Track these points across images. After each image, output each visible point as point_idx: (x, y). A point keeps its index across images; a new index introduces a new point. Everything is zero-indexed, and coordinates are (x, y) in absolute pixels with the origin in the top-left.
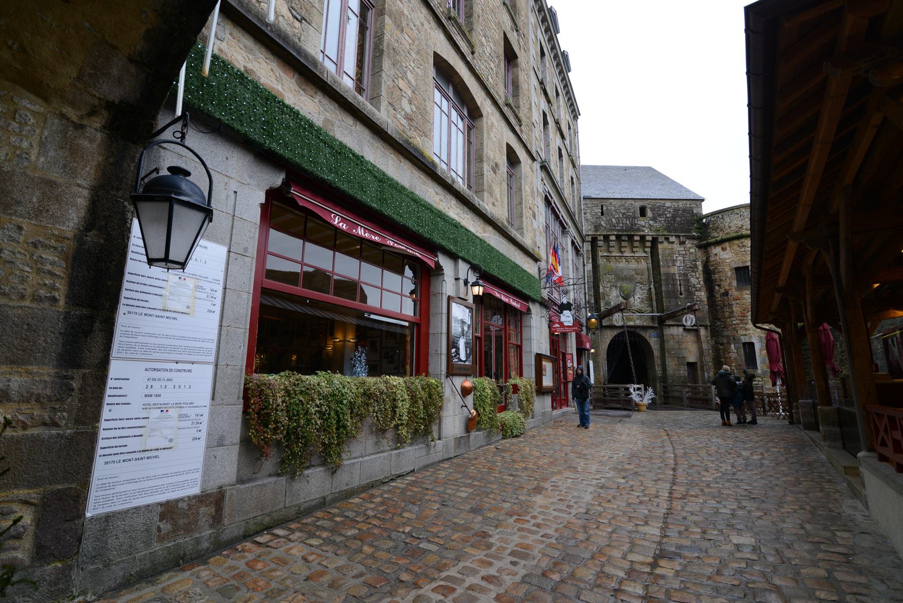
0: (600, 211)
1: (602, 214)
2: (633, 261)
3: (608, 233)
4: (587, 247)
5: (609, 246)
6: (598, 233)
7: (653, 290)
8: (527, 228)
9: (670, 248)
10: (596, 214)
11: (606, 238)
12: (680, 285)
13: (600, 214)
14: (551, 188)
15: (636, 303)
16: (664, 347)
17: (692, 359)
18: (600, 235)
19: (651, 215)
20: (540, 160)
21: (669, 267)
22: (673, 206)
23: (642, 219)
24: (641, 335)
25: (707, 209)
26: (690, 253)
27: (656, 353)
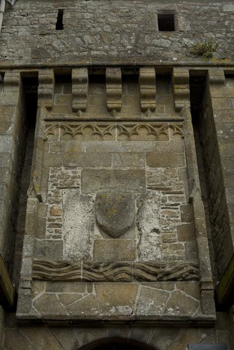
0: (55, 21)
1: (60, 26)
2: (143, 132)
13: (54, 27)
15: (144, 244)
18: (44, 67)
19: (188, 28)
23: (161, 33)
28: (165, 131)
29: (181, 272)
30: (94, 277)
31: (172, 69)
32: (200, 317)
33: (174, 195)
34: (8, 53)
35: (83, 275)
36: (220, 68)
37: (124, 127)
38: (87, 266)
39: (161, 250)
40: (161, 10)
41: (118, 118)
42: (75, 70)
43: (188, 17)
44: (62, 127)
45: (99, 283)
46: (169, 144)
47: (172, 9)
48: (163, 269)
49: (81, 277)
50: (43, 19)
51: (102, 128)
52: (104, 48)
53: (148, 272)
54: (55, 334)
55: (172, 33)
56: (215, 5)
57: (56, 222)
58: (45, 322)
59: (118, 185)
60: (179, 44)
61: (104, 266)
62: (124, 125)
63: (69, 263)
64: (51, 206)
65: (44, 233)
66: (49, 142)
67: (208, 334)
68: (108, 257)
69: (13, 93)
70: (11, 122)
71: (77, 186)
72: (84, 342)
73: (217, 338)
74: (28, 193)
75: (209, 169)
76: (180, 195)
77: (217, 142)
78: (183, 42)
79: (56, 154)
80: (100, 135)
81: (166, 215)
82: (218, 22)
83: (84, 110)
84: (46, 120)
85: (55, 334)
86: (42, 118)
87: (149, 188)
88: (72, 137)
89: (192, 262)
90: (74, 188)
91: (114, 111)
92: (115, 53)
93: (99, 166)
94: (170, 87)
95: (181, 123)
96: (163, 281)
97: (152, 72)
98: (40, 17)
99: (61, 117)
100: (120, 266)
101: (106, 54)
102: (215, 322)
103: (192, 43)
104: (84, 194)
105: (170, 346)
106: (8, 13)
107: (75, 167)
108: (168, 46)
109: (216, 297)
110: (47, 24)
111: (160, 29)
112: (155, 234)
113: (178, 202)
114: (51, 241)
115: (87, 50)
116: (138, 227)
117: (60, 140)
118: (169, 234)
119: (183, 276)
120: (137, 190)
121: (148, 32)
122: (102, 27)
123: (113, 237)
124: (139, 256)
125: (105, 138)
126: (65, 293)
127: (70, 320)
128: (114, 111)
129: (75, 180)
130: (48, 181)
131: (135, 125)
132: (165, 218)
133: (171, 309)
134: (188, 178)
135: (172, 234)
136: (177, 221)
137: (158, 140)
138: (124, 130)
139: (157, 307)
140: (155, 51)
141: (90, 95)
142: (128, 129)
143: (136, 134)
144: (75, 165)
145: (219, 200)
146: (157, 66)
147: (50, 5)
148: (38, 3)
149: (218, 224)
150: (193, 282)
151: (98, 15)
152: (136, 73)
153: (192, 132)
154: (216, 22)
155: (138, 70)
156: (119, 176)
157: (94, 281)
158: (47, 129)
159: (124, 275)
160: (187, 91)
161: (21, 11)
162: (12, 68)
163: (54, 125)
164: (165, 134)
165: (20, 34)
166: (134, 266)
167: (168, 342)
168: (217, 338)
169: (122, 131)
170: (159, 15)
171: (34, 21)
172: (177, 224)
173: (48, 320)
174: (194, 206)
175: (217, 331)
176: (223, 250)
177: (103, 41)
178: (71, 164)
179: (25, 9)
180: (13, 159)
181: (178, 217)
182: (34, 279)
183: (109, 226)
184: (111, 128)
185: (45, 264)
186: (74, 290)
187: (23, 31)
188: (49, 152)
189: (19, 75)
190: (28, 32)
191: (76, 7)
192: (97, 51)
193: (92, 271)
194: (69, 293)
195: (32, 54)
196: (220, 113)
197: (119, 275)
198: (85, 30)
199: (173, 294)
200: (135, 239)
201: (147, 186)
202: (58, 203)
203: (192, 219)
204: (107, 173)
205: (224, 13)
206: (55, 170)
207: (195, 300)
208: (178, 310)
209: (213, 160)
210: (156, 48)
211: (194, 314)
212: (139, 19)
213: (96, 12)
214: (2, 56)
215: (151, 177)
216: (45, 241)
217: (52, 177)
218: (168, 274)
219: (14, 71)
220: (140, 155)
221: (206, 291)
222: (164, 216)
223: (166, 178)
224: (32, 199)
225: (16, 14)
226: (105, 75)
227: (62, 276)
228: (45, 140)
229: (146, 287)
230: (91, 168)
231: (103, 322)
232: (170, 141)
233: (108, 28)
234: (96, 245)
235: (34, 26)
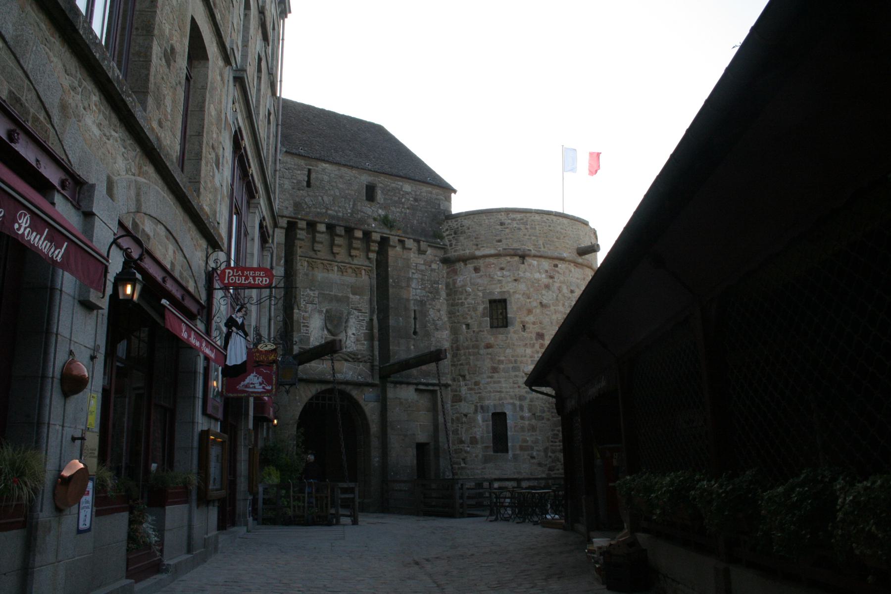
0: (306, 179)
1: (309, 184)
2: (350, 271)
3: (317, 219)
4: (279, 236)
5: (314, 241)
6: (299, 217)
8: (205, 182)
9: (405, 257)
10: (299, 182)
11: (312, 226)
12: (415, 318)
13: (305, 184)
14: (243, 119)
15: (348, 342)
17: (422, 438)
19: (382, 201)
20: (234, 66)
21: (402, 288)
22: (413, 193)
23: (367, 203)
25: (458, 205)
26: (432, 270)
27: (374, 428)
44: (307, 261)
53: (350, 357)
57: (306, 324)
64: (303, 314)
70: (282, 257)
71: (315, 302)
92: (340, 214)
93: (327, 291)
95: (370, 268)
107: (314, 290)
112: (352, 336)
114: (304, 336)
133: (360, 377)
136: (363, 330)
143: (346, 272)
154: (397, 198)
160: (377, 249)
161: (284, 164)
172: (363, 331)
178: (313, 288)
202: (306, 312)
205: (403, 191)
211: (370, 380)
217: (303, 295)
218: (358, 359)
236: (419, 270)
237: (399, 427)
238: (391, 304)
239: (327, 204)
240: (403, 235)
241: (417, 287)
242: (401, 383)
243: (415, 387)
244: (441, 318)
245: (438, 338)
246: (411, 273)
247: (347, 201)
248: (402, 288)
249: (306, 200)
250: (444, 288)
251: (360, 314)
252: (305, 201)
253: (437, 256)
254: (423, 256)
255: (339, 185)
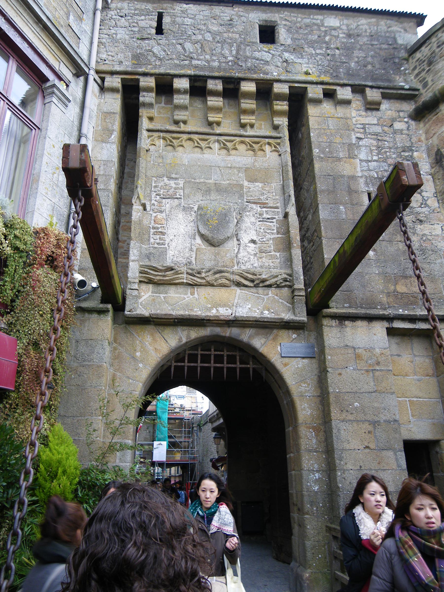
0: (155, 24)
1: (159, 30)
2: (242, 148)
7: (294, 219)
13: (154, 31)
16: (327, 388)
18: (145, 74)
19: (289, 41)
21: (339, 159)
22: (344, 27)
23: (262, 45)
24: (255, 350)
28: (263, 148)
29: (276, 279)
30: (197, 281)
31: (272, 84)
32: (292, 319)
33: (270, 209)
34: (107, 57)
35: (186, 279)
36: (319, 86)
37: (224, 141)
38: (190, 271)
39: (258, 260)
40: (263, 20)
41: (218, 132)
42: (176, 79)
43: (289, 30)
44: (164, 138)
45: (201, 287)
46: (266, 161)
47: (273, 20)
48: (260, 277)
49: (185, 281)
50: (143, 22)
51: (203, 142)
52: (205, 58)
53: (246, 279)
54: (160, 331)
55: (272, 46)
56: (317, 18)
57: (160, 230)
58: (152, 320)
59: (218, 197)
60: (280, 58)
61: (206, 272)
62: (224, 140)
63: (174, 268)
64: (155, 214)
65: (149, 240)
66: (151, 153)
67: (298, 335)
68: (208, 264)
69: (114, 100)
70: (113, 130)
71: (179, 197)
72: (187, 339)
73: (306, 338)
74: (133, 201)
75: (301, 189)
76: (276, 210)
77: (312, 160)
78: (283, 56)
79: (159, 165)
80: (201, 148)
81: (262, 228)
82: (319, 37)
83: (185, 122)
84: (148, 130)
85: (160, 331)
86: (145, 128)
87: (247, 202)
88: (175, 149)
89: (286, 272)
90: (177, 198)
91: (215, 124)
92: (216, 64)
93: (200, 178)
94: (268, 104)
95: (278, 141)
96: (259, 287)
97: (253, 86)
98: (139, 19)
99: (163, 128)
100: (221, 272)
101: (207, 64)
102: (306, 325)
103: (292, 58)
104: (186, 205)
105: (264, 343)
106: (105, 12)
107: (176, 179)
108: (268, 60)
109: (307, 303)
110: (147, 28)
111: (262, 41)
112: (252, 245)
113: (274, 217)
114: (156, 248)
115: (188, 59)
116: (237, 238)
117: (162, 151)
118: (265, 245)
119: (278, 283)
120: (236, 203)
121: (250, 44)
122: (202, 35)
123: (214, 246)
124: (238, 264)
125: (205, 151)
126: (169, 295)
127: (175, 319)
128: (215, 124)
129: (176, 191)
130: (151, 191)
131: (234, 140)
132: (262, 231)
133: (266, 312)
134: (284, 194)
135: (268, 245)
137: (256, 157)
138: (224, 144)
139: (254, 309)
140: (256, 65)
141: (191, 108)
142: (228, 144)
143: (236, 149)
144: (176, 176)
145: (310, 217)
146: (258, 80)
147: (149, 6)
148: (136, 3)
149: (308, 239)
150: (286, 289)
151: (199, 21)
152: (237, 87)
153: (289, 150)
154: (316, 37)
155: (239, 83)
156: (219, 189)
157: (196, 285)
158: (149, 140)
159: (224, 281)
160: (286, 108)
162: (112, 73)
163: (156, 136)
164: (263, 150)
165: (119, 36)
166: (233, 273)
167: (263, 341)
168: (306, 338)
169: (222, 145)
170: (260, 26)
171: (132, 23)
172: (273, 236)
173: (155, 318)
174: (290, 220)
175: (306, 332)
176: (312, 263)
177: (204, 51)
178: (173, 176)
179: (122, 9)
180: (116, 167)
181: (273, 230)
182: (140, 282)
183: (210, 235)
184: (212, 142)
185: (151, 268)
186: (177, 293)
187: (122, 34)
188: (152, 162)
189: (120, 81)
190: (127, 35)
191: (176, 11)
192: (198, 60)
193: (194, 276)
194: (174, 295)
195: (132, 60)
196: (317, 132)
197: (220, 280)
198: (185, 37)
199: (268, 299)
200: (234, 249)
201: (245, 200)
202: (161, 212)
203: (287, 232)
204: (208, 186)
206: (158, 181)
207: (288, 305)
208: (273, 313)
209: (306, 179)
210: (258, 62)
211: (287, 316)
212: (241, 28)
213: (197, 17)
214: (101, 59)
215: (249, 192)
216: (150, 247)
217: (155, 187)
218: (263, 281)
219: (114, 76)
220: (239, 169)
221: (298, 297)
222: (261, 229)
223: (264, 193)
224: (137, 207)
225: (113, 14)
226: (205, 87)
227: (167, 280)
228: (147, 151)
229: (243, 291)
230: (193, 180)
231: (205, 321)
232: (267, 158)
233: (209, 37)
234: (198, 253)
235: (133, 29)
236: (370, 134)
237: (356, 404)
238: (321, 185)
239: (191, 53)
240: (331, 81)
241: (370, 158)
242: (354, 318)
243: (386, 324)
244: (425, 204)
245: (424, 235)
246: (354, 137)
247: (226, 46)
248: (339, 159)
249: (155, 51)
250: (425, 156)
251: (263, 209)
252: (153, 52)
253: (402, 111)
254: (374, 113)
255: (210, 27)
